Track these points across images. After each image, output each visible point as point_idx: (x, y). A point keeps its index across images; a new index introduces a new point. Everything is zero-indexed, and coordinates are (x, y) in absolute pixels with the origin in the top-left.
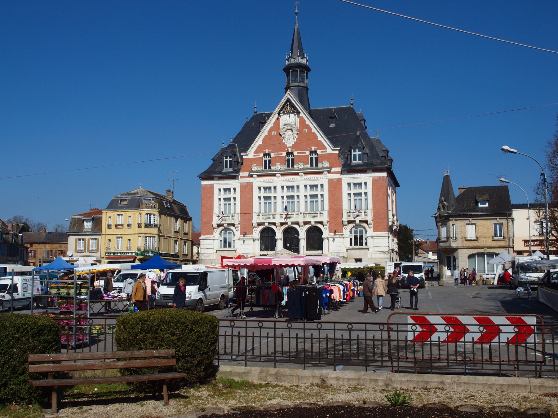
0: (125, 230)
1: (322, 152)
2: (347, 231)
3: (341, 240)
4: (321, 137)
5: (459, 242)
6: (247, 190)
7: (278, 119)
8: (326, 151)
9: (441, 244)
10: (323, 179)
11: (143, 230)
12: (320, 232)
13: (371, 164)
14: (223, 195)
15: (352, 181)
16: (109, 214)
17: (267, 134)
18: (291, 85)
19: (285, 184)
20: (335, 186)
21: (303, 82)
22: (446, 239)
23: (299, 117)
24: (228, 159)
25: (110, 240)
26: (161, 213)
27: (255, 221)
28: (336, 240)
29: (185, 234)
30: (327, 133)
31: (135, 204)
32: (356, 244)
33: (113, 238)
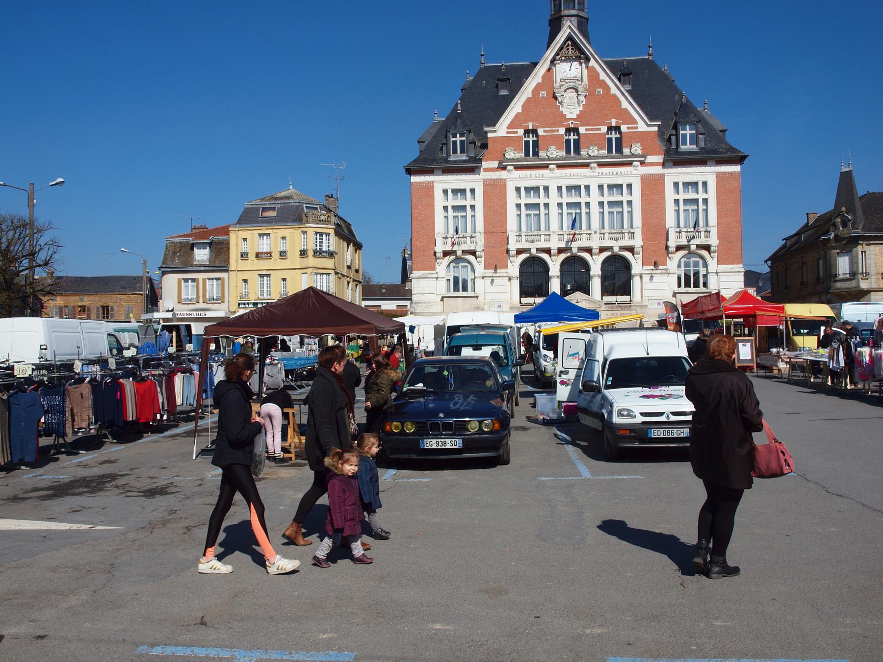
0: (276, 262)
1: (628, 128)
2: (674, 262)
3: (664, 278)
4: (627, 104)
5: (873, 280)
6: (495, 193)
7: (549, 70)
8: (637, 128)
9: (839, 285)
10: (631, 175)
11: (311, 261)
12: (627, 266)
13: (715, 152)
14: (452, 202)
15: (681, 180)
16: (242, 234)
17: (530, 95)
18: (563, 13)
19: (565, 183)
20: (652, 188)
21: (583, 10)
22: (848, 276)
23: (587, 67)
24: (458, 139)
25: (245, 281)
26: (337, 234)
27: (513, 246)
28: (656, 278)
29: (357, 271)
30: (637, 96)
31: (293, 215)
32: (687, 285)
33: (254, 278)
